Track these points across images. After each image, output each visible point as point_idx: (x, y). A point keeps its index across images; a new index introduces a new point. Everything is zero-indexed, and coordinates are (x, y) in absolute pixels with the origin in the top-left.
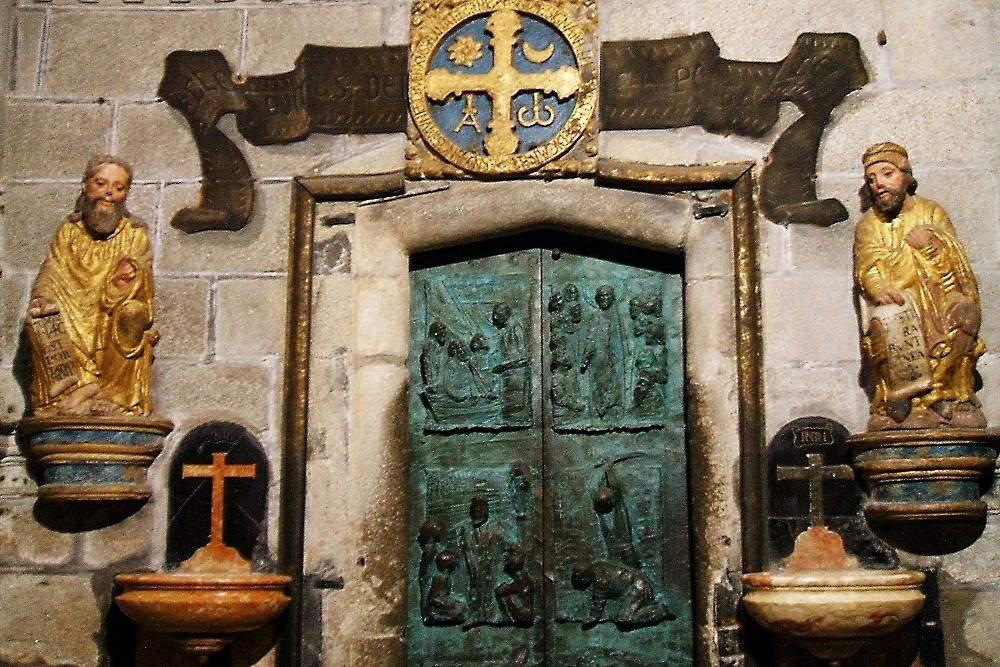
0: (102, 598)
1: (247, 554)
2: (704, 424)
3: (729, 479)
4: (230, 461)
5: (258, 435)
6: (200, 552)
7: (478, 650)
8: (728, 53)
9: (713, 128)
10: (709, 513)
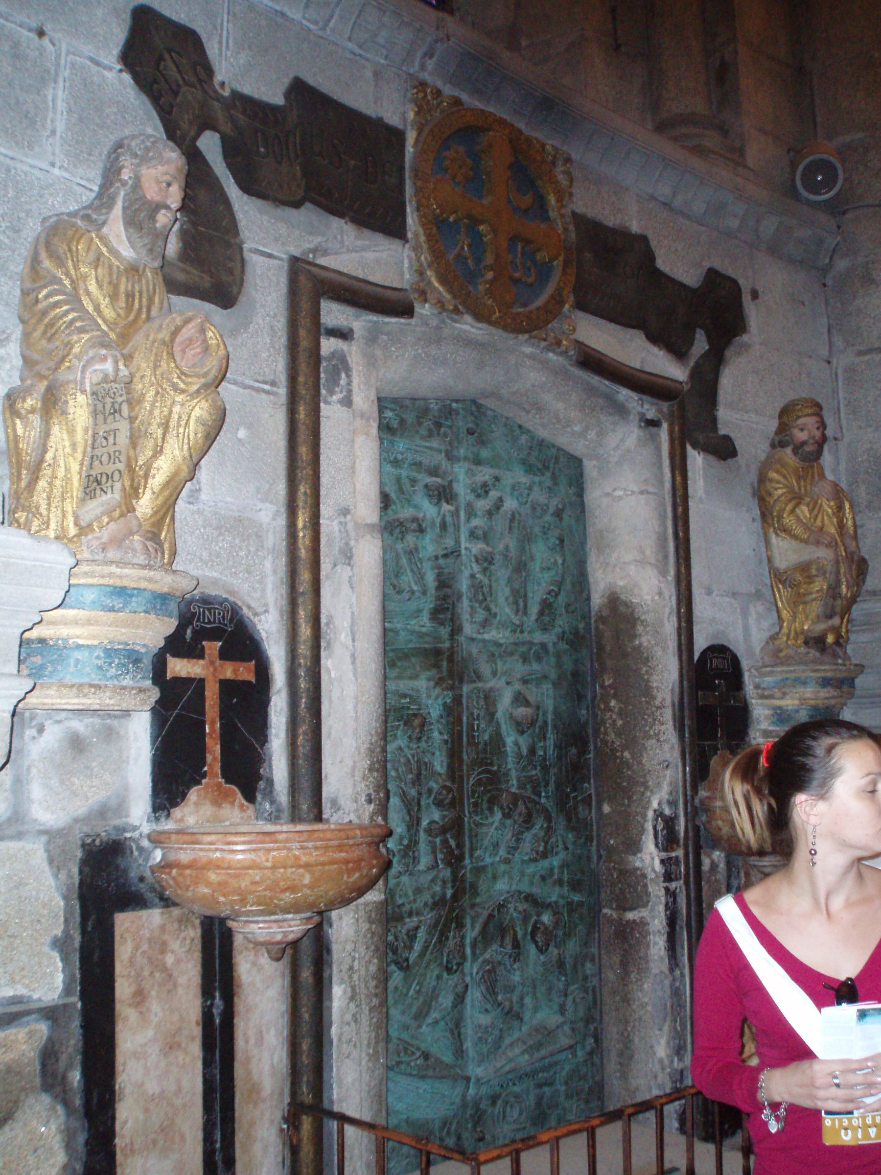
0: (63, 876)
1: (250, 797)
2: (645, 644)
3: (668, 702)
4: (225, 655)
5: (256, 620)
6: (193, 794)
7: (399, 906)
8: (662, 264)
9: (653, 339)
10: (650, 737)
